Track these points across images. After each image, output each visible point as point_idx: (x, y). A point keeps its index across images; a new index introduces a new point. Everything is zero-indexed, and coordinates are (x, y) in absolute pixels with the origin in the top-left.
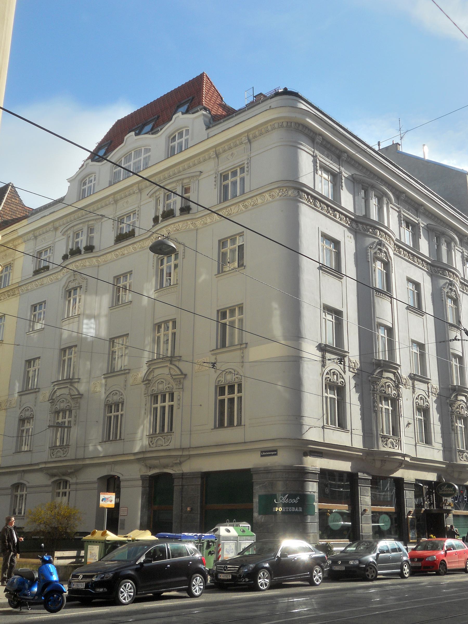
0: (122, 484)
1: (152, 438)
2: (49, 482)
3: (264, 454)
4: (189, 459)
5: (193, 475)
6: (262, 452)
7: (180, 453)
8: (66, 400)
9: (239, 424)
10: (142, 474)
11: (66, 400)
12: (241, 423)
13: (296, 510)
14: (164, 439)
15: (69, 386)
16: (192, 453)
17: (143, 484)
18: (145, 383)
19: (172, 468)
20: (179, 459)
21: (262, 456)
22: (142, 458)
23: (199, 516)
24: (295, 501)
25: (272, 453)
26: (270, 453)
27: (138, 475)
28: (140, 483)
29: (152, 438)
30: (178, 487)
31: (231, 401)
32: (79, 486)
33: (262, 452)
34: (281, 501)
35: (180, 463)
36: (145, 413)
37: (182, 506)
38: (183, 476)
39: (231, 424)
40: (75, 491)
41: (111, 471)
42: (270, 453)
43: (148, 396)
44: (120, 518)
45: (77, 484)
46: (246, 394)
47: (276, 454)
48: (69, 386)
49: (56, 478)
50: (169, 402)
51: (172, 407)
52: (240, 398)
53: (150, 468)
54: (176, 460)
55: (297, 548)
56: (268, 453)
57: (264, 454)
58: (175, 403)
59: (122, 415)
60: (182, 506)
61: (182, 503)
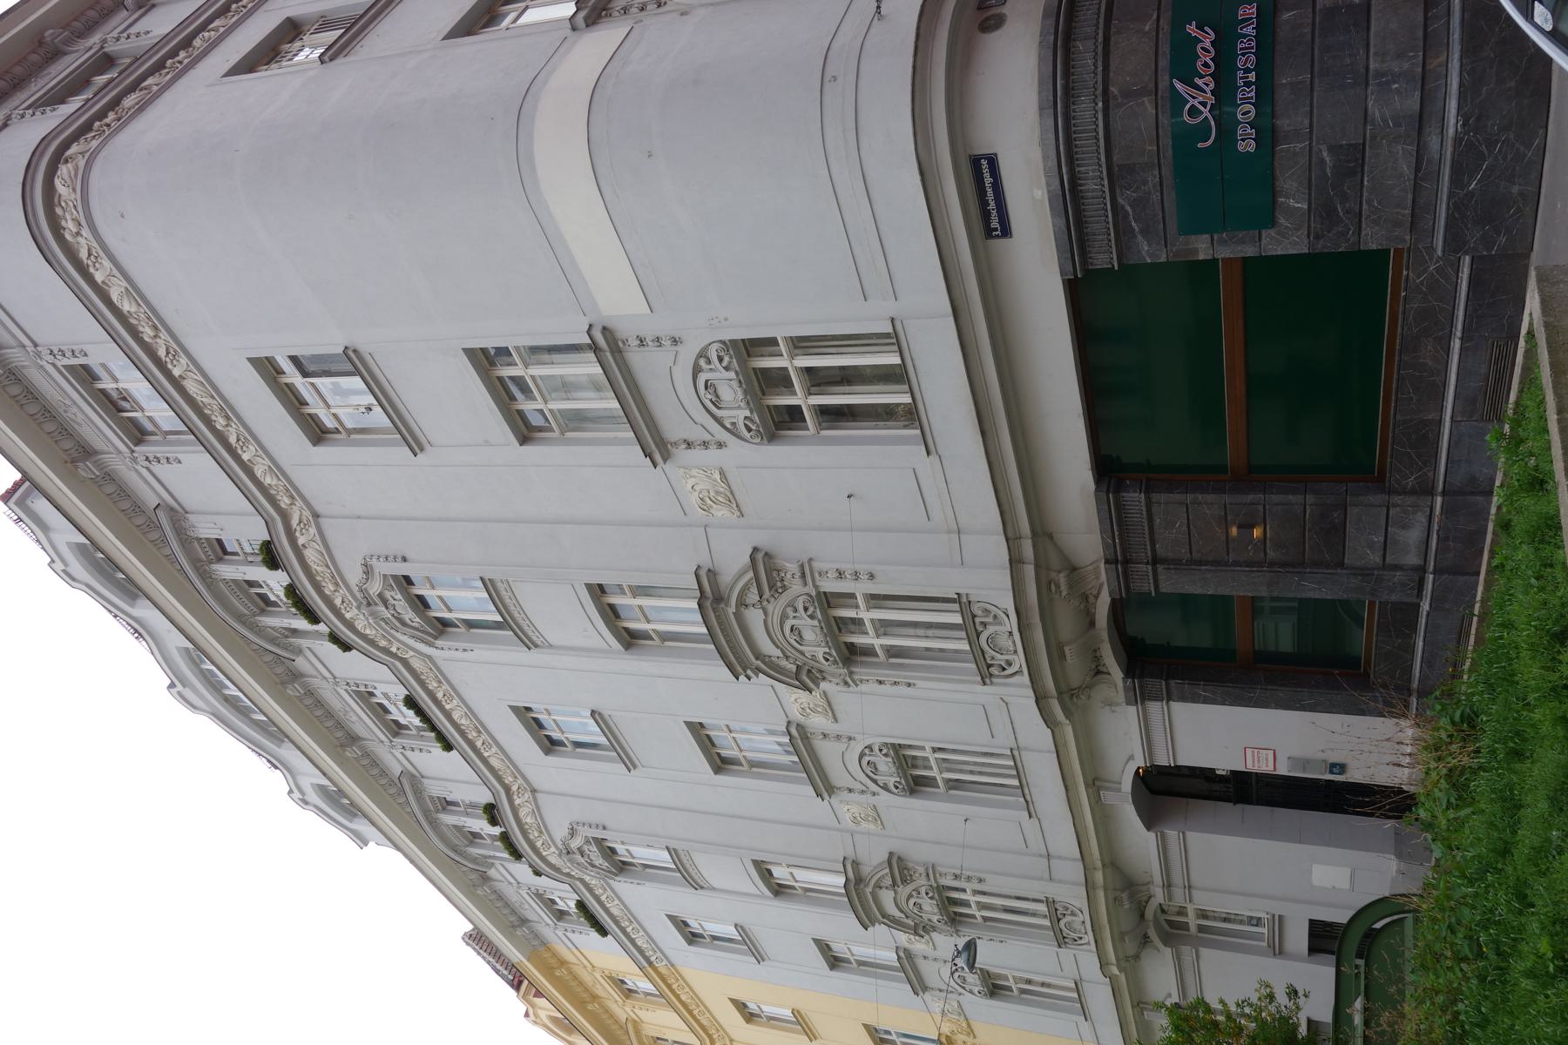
0: (1163, 760)
1: (989, 666)
2: (1168, 952)
3: (995, 224)
4: (1051, 537)
5: (1116, 522)
6: (989, 233)
7: (1029, 571)
8: (910, 896)
9: (892, 339)
10: (1121, 697)
11: (910, 896)
12: (887, 335)
13: (1250, 30)
14: (984, 625)
15: (869, 890)
16: (1025, 526)
17: (1158, 698)
18: (811, 685)
19: (1091, 599)
20: (1053, 575)
21: (1006, 232)
22: (1063, 699)
23: (1276, 498)
24: (1207, 44)
25: (988, 180)
26: (990, 192)
27: (1129, 716)
28: (1155, 708)
29: (989, 666)
30: (1161, 577)
31: (818, 379)
32: (1177, 878)
33: (989, 233)
34: (1206, 112)
35: (1073, 570)
36: (909, 685)
37: (1236, 563)
38: (1120, 560)
39: (895, 376)
40: (1194, 892)
41: (1119, 790)
42: (990, 192)
43: (851, 673)
44: (1283, 770)
45: (1168, 885)
46: (778, 320)
47: (993, 161)
48: (869, 890)
49: (1152, 934)
50: (857, 607)
51: (876, 600)
52: (801, 344)
53: (1098, 672)
54: (1058, 586)
55: (1507, 428)
56: (992, 205)
57: (995, 224)
58: (861, 589)
59: (935, 750)
60: (1236, 563)
61: (1226, 564)
